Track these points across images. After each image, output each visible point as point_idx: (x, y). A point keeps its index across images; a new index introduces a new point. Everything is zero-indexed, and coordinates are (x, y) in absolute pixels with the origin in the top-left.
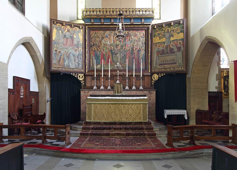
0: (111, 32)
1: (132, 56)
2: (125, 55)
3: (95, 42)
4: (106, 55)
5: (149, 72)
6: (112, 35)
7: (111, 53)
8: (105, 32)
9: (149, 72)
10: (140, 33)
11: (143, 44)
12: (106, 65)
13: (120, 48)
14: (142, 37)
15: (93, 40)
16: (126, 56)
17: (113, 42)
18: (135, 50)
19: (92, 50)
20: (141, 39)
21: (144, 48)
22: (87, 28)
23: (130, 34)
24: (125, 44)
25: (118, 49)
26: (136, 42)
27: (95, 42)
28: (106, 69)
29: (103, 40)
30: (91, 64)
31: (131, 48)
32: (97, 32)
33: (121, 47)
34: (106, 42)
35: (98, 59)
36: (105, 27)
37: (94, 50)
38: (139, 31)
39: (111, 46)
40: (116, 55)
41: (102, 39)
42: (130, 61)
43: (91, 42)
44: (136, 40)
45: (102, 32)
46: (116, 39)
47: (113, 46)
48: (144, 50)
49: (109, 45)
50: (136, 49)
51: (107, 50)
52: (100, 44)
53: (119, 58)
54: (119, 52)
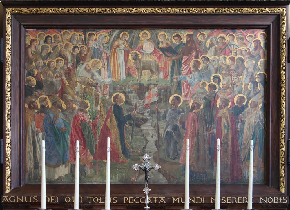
0: (118, 37)
1: (208, 129)
2: (175, 128)
3: (44, 73)
4: (94, 125)
5: (283, 191)
6: (122, 47)
7: (114, 119)
8: (90, 35)
9: (282, 195)
10: (241, 39)
11: (255, 84)
12: (93, 165)
13: (155, 99)
14: (251, 56)
15: (37, 67)
16: (181, 130)
17: (123, 76)
18: (221, 108)
19: (33, 107)
20: (249, 64)
21: (259, 99)
22: (8, 16)
23: (201, 42)
24: (179, 83)
25: (147, 102)
26: (224, 75)
27: (44, 73)
28: (96, 180)
29: (81, 70)
30: (27, 160)
31: (205, 98)
32: (53, 33)
33: (159, 94)
34: (93, 75)
35: (59, 143)
36: (91, 14)
37: (43, 107)
38: (240, 32)
39: (115, 90)
40: (138, 126)
41: (78, 62)
42: (198, 150)
43: (30, 74)
44: (224, 66)
45: (78, 36)
46: (136, 64)
47: (124, 92)
48: (260, 106)
49: (106, 86)
50: (225, 103)
51: (97, 105)
52: (67, 83)
53: (149, 138)
54: (152, 113)
